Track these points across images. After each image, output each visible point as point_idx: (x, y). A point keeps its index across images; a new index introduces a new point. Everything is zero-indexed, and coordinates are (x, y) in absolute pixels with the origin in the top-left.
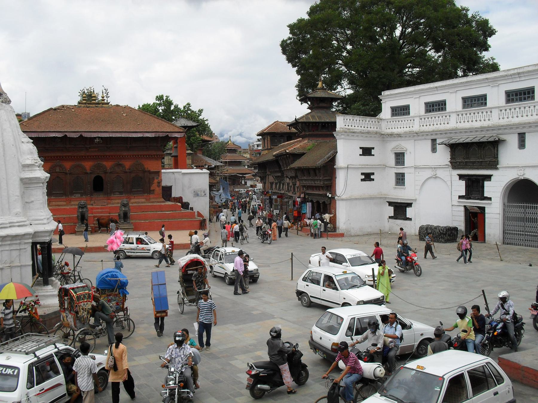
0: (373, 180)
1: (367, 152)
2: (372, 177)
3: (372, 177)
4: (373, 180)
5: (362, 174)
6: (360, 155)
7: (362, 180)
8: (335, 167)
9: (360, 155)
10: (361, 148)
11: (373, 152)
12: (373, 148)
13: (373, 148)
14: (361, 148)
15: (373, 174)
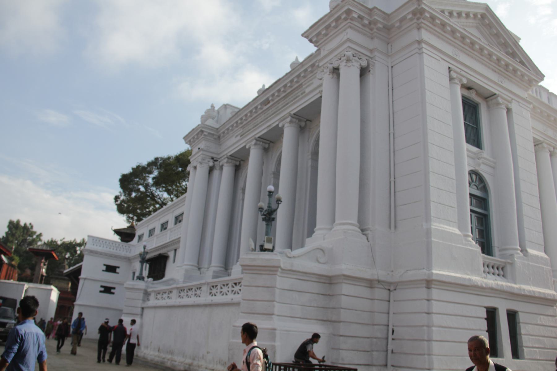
0: (113, 293)
1: (111, 269)
2: (112, 291)
3: (112, 291)
4: (113, 293)
5: (102, 286)
6: (103, 271)
7: (101, 292)
8: (80, 277)
9: (103, 271)
10: (105, 265)
11: (118, 270)
12: (119, 267)
13: (119, 267)
14: (105, 265)
15: (114, 288)
